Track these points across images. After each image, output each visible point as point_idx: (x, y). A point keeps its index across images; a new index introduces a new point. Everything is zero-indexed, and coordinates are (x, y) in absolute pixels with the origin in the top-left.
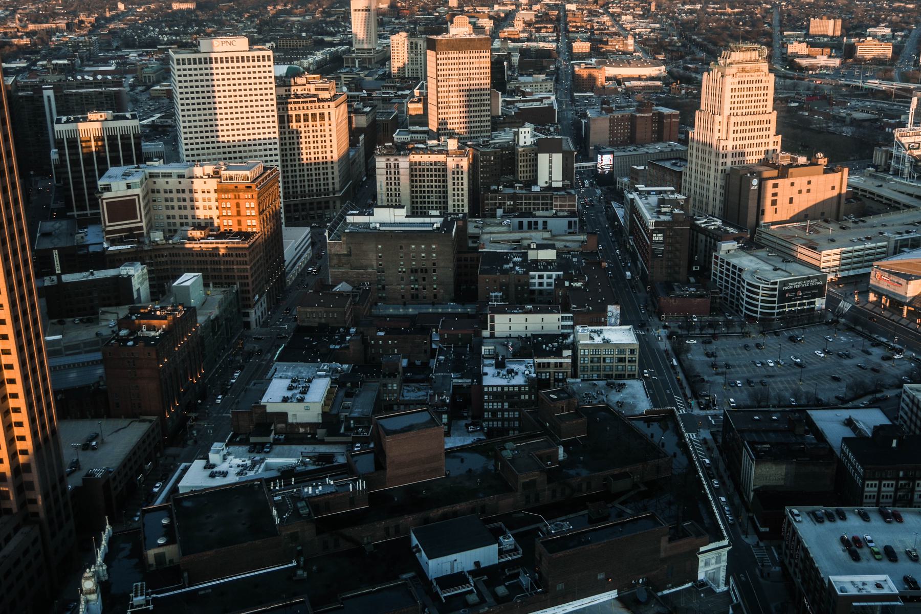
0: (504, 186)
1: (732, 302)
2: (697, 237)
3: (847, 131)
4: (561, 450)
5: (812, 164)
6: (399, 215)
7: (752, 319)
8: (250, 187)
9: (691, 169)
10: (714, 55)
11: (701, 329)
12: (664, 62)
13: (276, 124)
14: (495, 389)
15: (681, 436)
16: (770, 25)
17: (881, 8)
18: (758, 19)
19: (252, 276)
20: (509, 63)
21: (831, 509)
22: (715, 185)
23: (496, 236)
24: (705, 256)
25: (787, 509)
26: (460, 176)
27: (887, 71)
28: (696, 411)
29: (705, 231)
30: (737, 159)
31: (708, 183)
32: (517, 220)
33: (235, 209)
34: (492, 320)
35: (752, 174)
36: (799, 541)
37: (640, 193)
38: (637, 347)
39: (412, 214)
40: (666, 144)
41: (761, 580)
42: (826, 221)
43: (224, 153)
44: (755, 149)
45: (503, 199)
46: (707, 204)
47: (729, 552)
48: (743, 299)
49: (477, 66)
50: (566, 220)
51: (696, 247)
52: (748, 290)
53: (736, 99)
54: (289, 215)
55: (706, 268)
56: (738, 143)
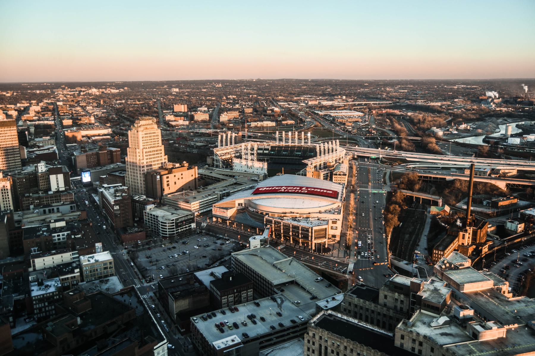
0: (33, 194)
1: (155, 232)
3: (195, 151)
4: (79, 319)
5: (182, 167)
7: (165, 238)
9: (128, 174)
10: (133, 123)
11: (143, 246)
12: (110, 127)
14: (39, 297)
16: (157, 108)
17: (202, 100)
18: (151, 106)
20: (29, 132)
22: (141, 180)
23: (31, 219)
27: (208, 125)
28: (146, 284)
30: (149, 168)
31: (137, 180)
32: (42, 210)
34: (34, 262)
35: (156, 173)
37: (105, 188)
38: (112, 261)
40: (115, 165)
41: (185, 353)
42: (191, 190)
44: (156, 163)
45: (33, 199)
46: (138, 189)
49: (9, 134)
50: (69, 207)
52: (162, 225)
53: (145, 142)
55: (141, 218)
56: (148, 160)
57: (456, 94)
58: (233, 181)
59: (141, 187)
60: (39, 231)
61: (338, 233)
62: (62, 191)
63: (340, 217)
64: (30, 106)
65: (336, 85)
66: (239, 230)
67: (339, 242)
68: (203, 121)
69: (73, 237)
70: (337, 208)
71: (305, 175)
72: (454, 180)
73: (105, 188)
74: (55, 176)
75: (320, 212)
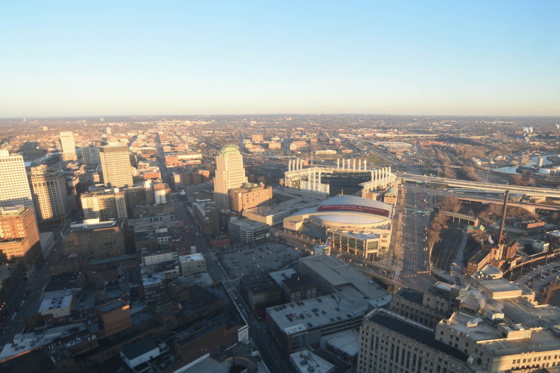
15: (225, 290)
21: (281, 306)
25: (267, 309)
28: (230, 281)
29: (224, 214)
36: (272, 319)
47: (249, 329)
55: (226, 228)
57: (495, 129)
58: (301, 199)
60: (147, 235)
61: (387, 245)
62: (164, 204)
63: (390, 232)
64: (138, 134)
65: (389, 119)
66: (305, 240)
67: (388, 253)
68: (277, 149)
69: (173, 240)
70: (388, 225)
71: (361, 196)
72: (489, 204)
73: (198, 202)
75: (373, 228)
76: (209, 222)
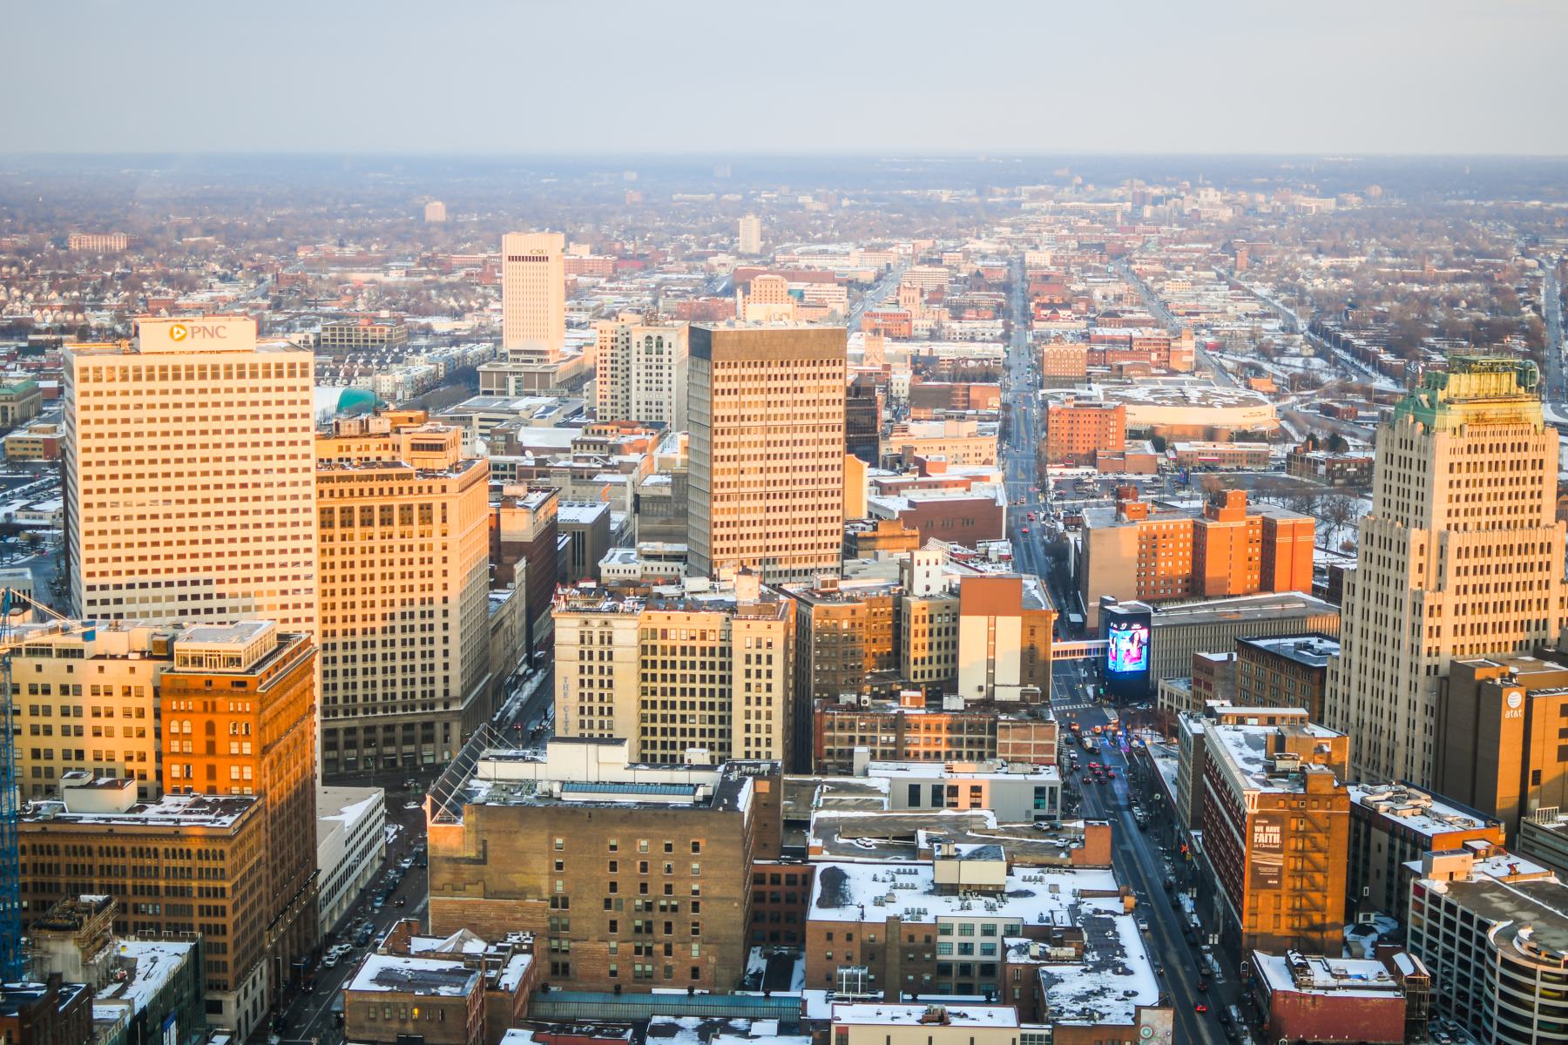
2: (1368, 835)
6: (613, 763)
8: (242, 684)
13: (314, 530)
19: (235, 908)
22: (1412, 705)
24: (1390, 887)
26: (764, 667)
33: (202, 738)
39: (645, 760)
43: (182, 598)
46: (1391, 754)
48: (1491, 1004)
49: (813, 396)
51: (1366, 862)
53: (1463, 491)
54: (332, 754)
59: (1410, 742)
62: (1007, 707)
74: (982, 621)
76: (1277, 861)
